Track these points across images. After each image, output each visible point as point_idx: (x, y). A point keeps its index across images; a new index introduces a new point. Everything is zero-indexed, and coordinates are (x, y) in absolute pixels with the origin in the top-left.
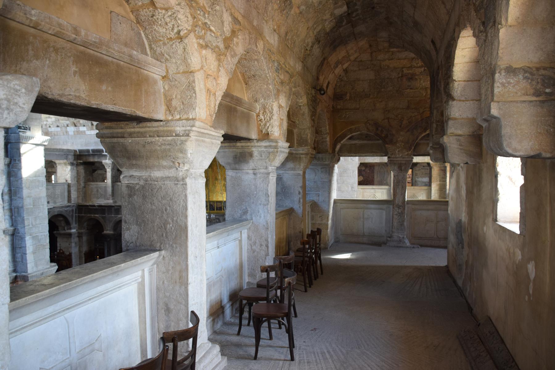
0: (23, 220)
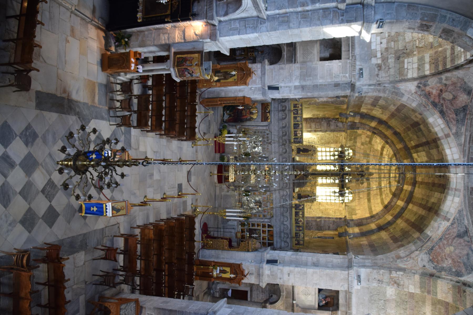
0: (275, 30)
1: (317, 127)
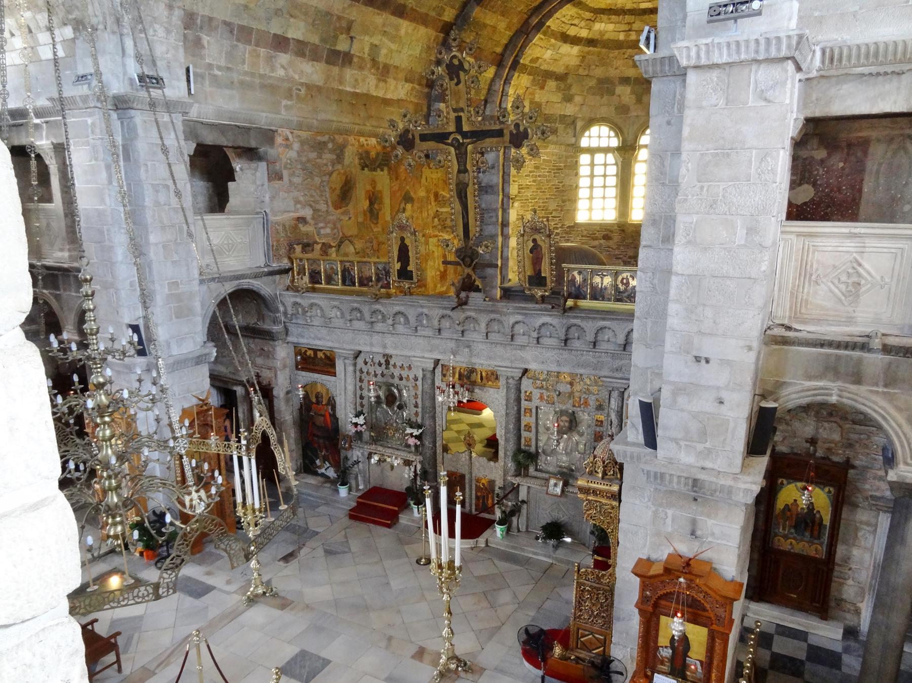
1: (494, 219)
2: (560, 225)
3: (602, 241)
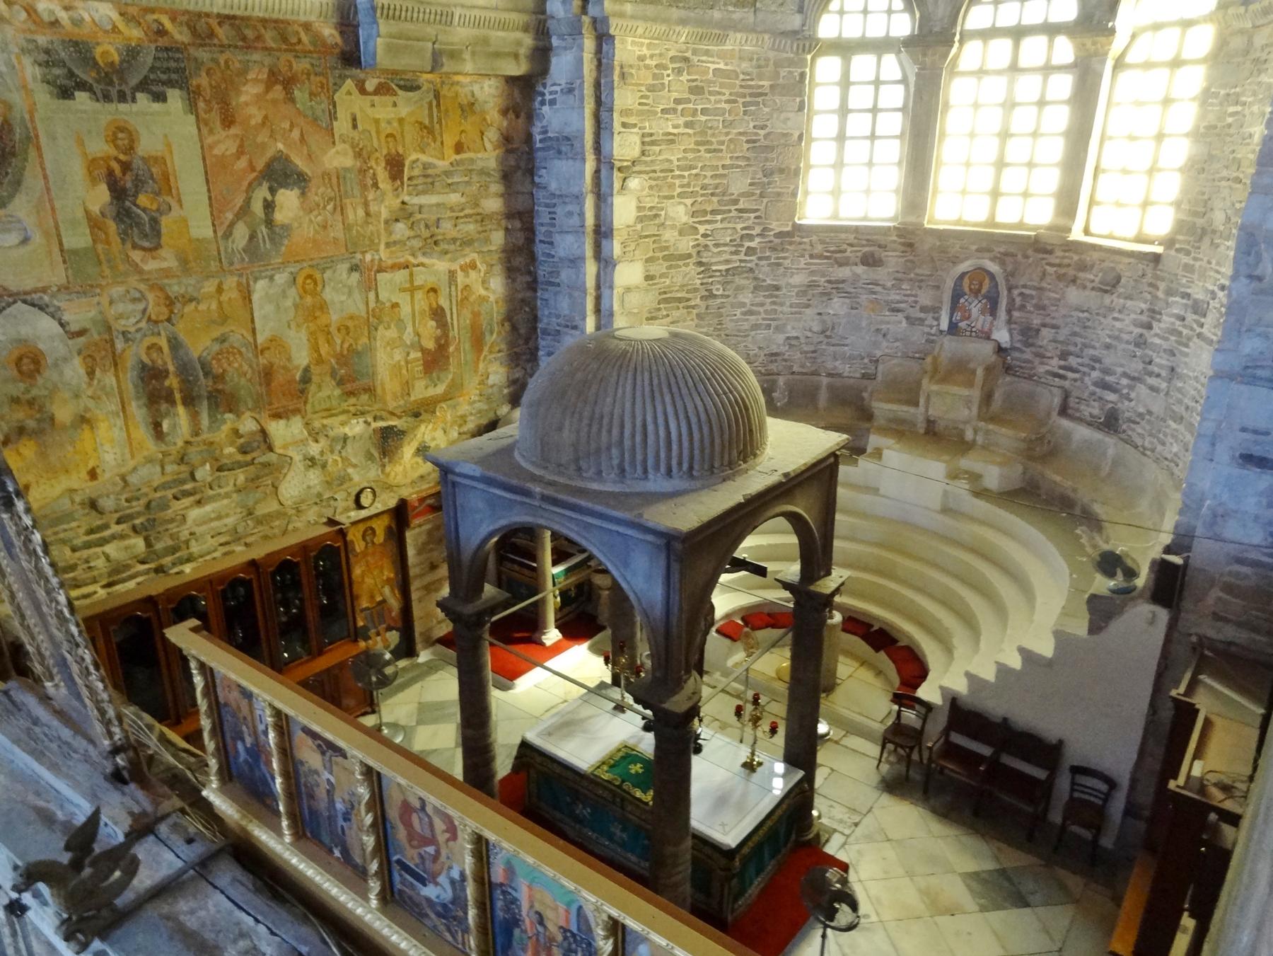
1: (575, 221)
2: (758, 230)
3: (860, 269)
